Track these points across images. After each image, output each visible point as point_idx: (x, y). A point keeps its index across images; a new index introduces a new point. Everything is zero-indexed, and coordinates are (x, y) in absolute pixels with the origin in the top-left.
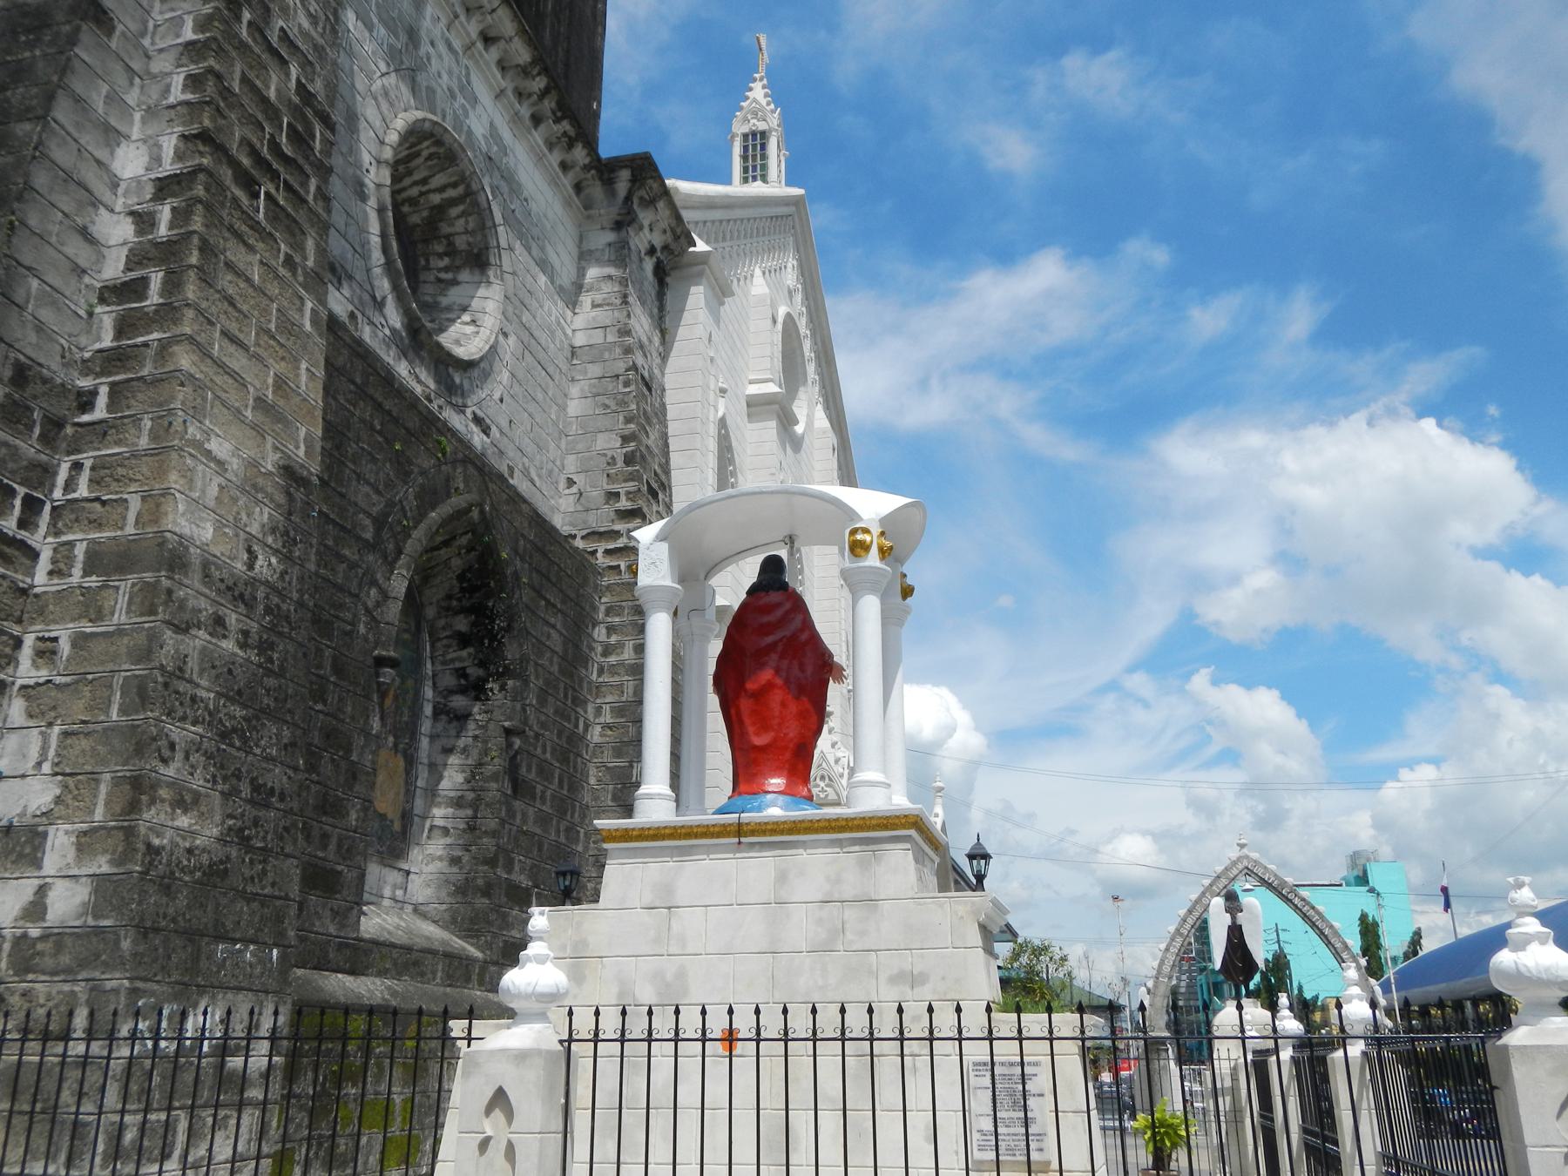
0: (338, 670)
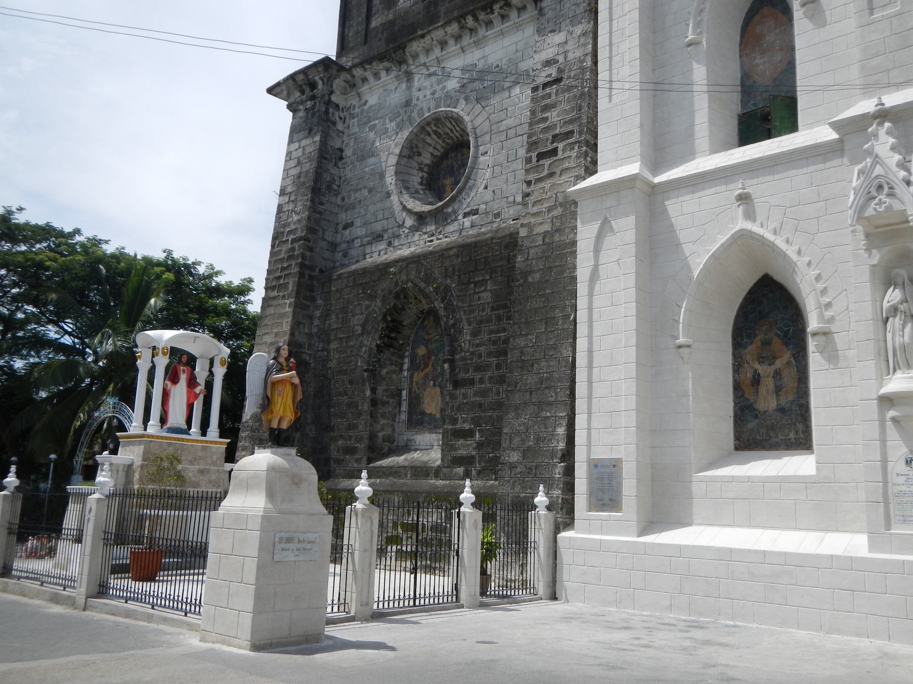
0: (351, 382)
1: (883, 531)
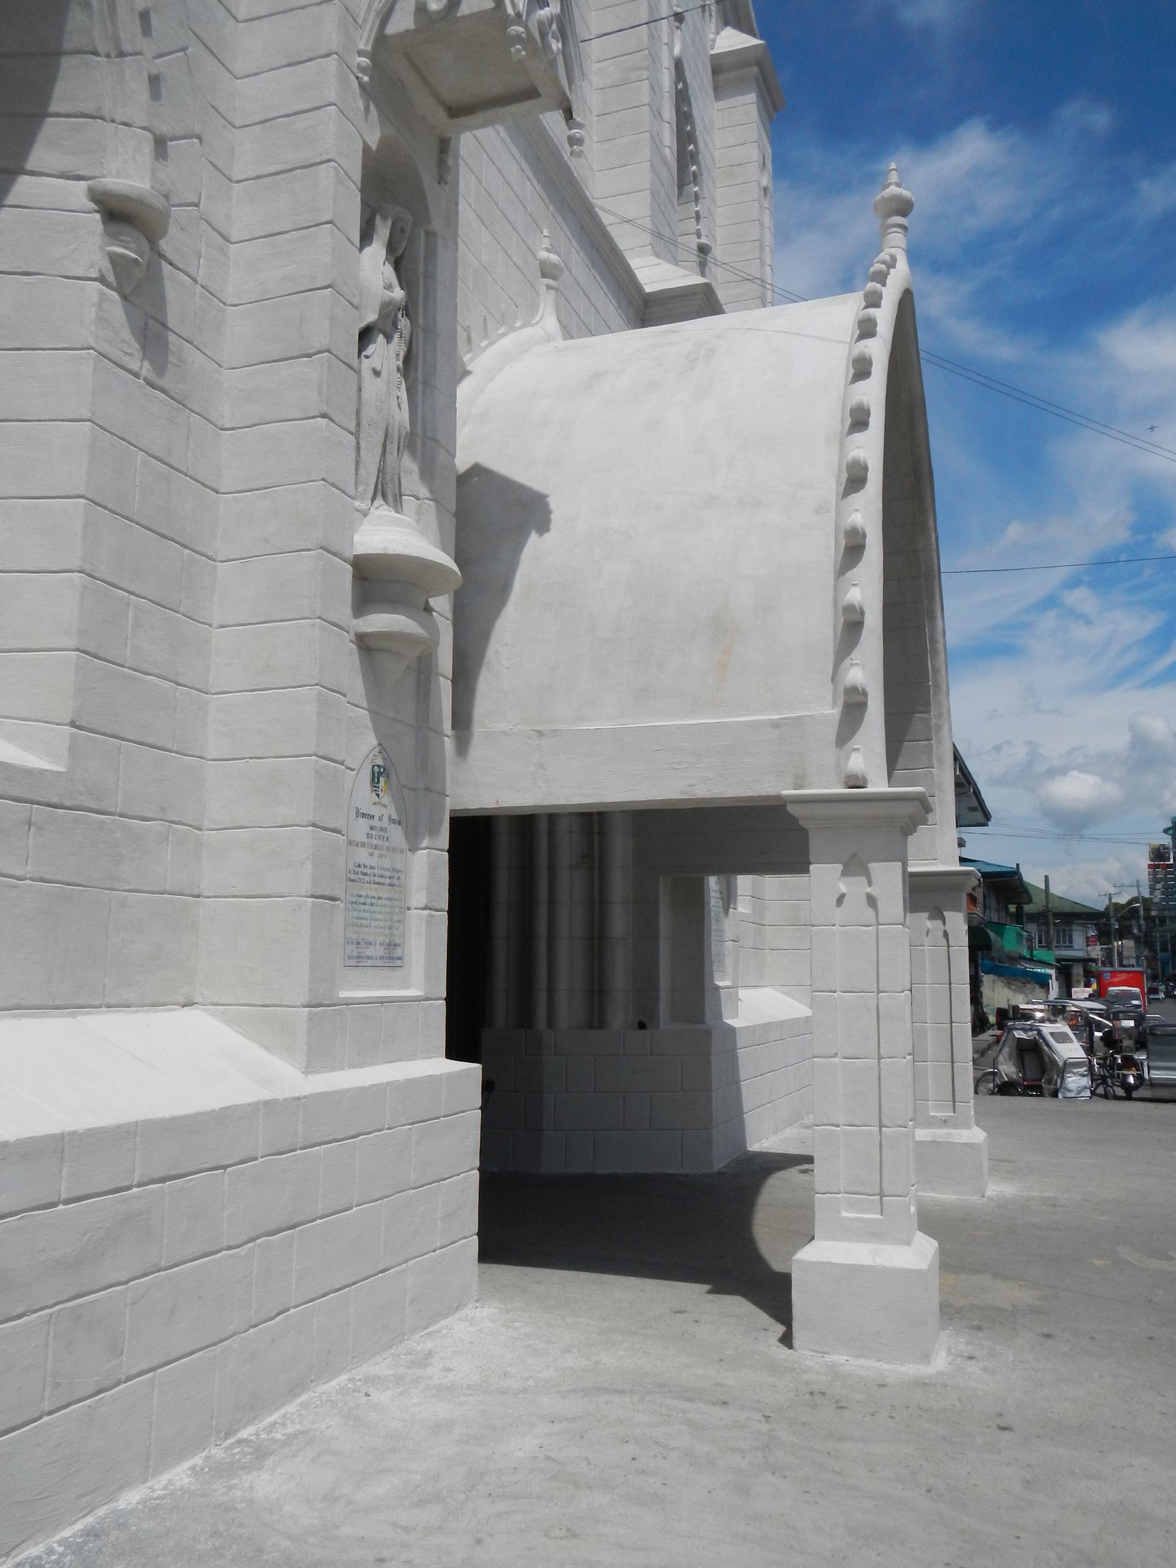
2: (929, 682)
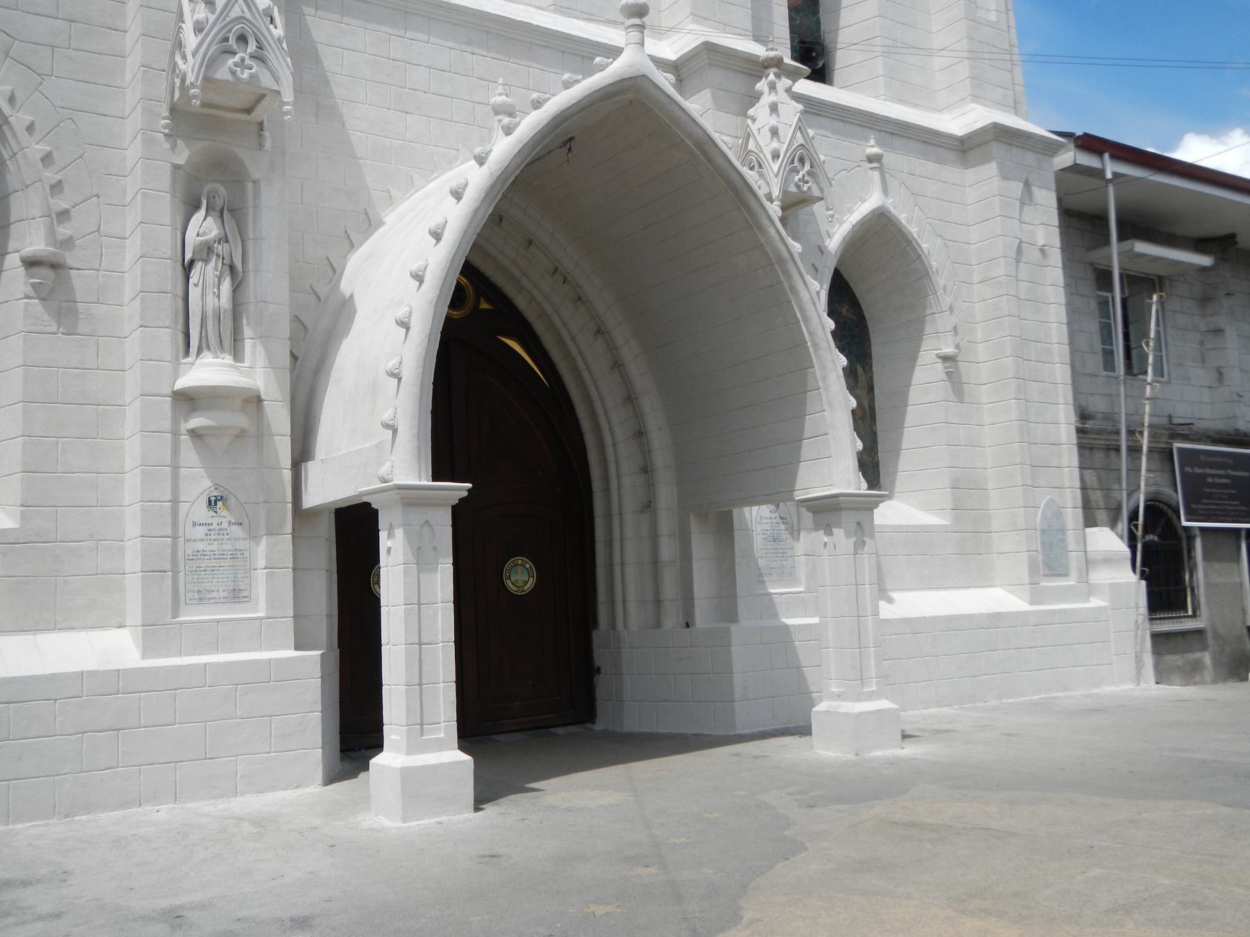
1: (169, 619)
2: (807, 343)
